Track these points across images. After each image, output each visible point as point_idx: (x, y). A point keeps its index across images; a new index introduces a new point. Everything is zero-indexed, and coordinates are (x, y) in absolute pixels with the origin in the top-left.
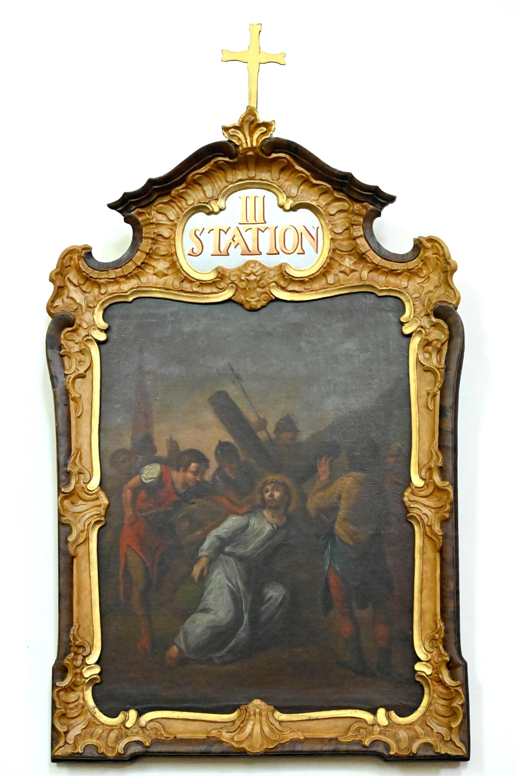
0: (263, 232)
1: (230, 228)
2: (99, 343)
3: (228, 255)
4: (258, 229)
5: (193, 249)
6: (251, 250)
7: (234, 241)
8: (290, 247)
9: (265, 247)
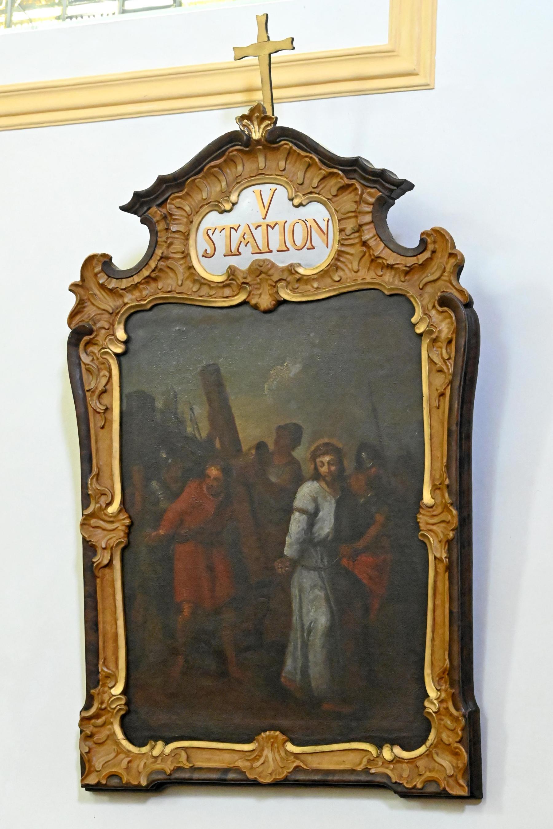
1: (240, 226)
3: (240, 254)
4: (268, 226)
5: (206, 250)
6: (261, 249)
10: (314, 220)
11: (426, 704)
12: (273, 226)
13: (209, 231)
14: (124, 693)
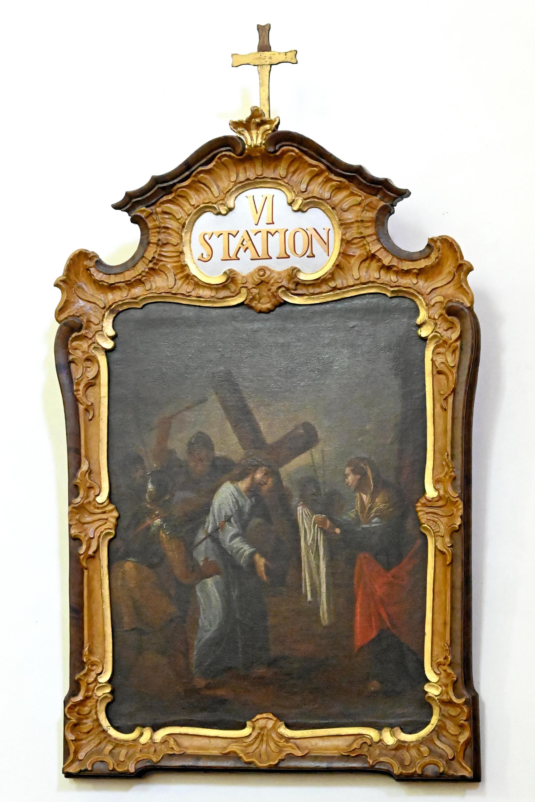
0: (273, 235)
2: (107, 352)
3: (239, 259)
4: (268, 232)
5: (202, 254)
7: (243, 245)
8: (300, 250)
9: (274, 251)
10: (314, 229)
11: (427, 688)
12: (273, 234)
13: (206, 235)
14: (110, 681)
